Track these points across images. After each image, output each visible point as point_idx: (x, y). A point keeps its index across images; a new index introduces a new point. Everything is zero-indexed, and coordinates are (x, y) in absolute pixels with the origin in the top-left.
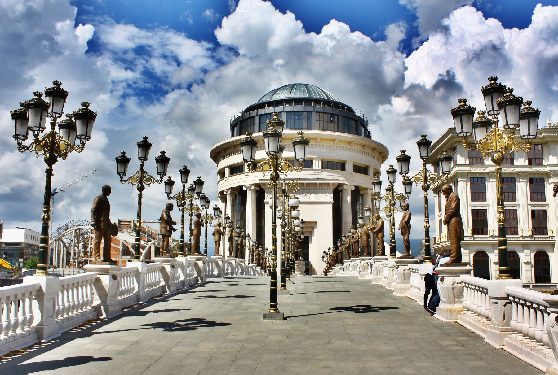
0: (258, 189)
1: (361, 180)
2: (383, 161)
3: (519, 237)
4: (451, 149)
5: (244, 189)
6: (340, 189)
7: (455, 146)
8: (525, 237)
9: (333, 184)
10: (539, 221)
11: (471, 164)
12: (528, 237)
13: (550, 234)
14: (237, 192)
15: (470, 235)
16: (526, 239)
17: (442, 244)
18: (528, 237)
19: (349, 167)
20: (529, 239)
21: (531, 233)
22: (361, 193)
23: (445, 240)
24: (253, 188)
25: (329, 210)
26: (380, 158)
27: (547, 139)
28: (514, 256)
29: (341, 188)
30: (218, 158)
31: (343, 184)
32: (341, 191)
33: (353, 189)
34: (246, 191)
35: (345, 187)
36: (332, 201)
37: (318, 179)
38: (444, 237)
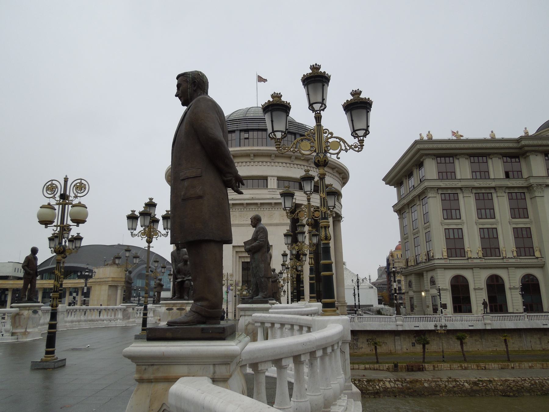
2: (344, 184)
3: (503, 259)
4: (416, 165)
7: (421, 160)
8: (509, 258)
10: (524, 240)
11: (440, 179)
12: (511, 258)
13: (537, 254)
15: (446, 257)
16: (511, 260)
17: (410, 268)
18: (511, 258)
20: (513, 260)
21: (515, 254)
23: (413, 264)
26: (341, 179)
27: (526, 148)
28: (497, 281)
37: (273, 199)
38: (412, 261)
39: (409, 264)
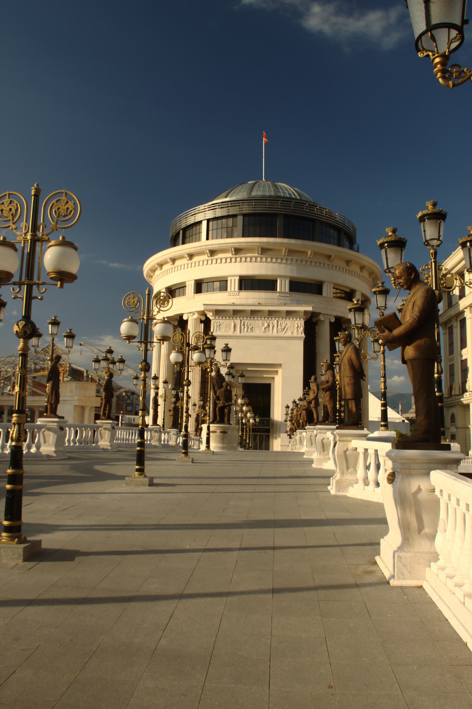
0: (203, 318)
1: (343, 309)
5: (185, 318)
6: (314, 320)
9: (306, 312)
14: (176, 323)
19: (327, 290)
22: (344, 326)
23: (457, 393)
24: (196, 316)
25: (298, 349)
26: (371, 280)
29: (317, 319)
30: (154, 277)
31: (319, 314)
32: (316, 323)
33: (333, 320)
34: (187, 321)
35: (321, 318)
36: (303, 335)
38: (457, 389)
39: (453, 393)
